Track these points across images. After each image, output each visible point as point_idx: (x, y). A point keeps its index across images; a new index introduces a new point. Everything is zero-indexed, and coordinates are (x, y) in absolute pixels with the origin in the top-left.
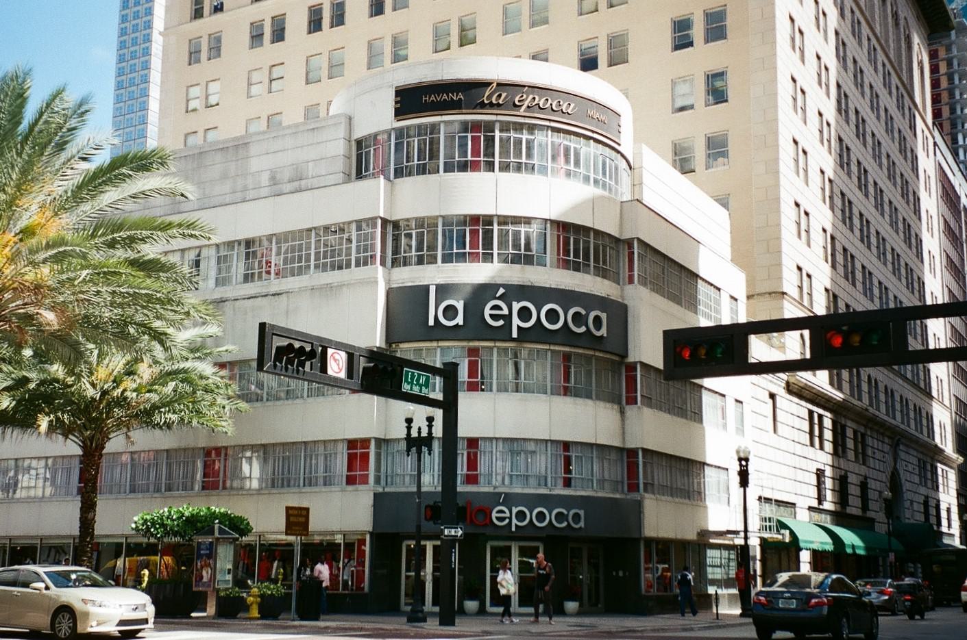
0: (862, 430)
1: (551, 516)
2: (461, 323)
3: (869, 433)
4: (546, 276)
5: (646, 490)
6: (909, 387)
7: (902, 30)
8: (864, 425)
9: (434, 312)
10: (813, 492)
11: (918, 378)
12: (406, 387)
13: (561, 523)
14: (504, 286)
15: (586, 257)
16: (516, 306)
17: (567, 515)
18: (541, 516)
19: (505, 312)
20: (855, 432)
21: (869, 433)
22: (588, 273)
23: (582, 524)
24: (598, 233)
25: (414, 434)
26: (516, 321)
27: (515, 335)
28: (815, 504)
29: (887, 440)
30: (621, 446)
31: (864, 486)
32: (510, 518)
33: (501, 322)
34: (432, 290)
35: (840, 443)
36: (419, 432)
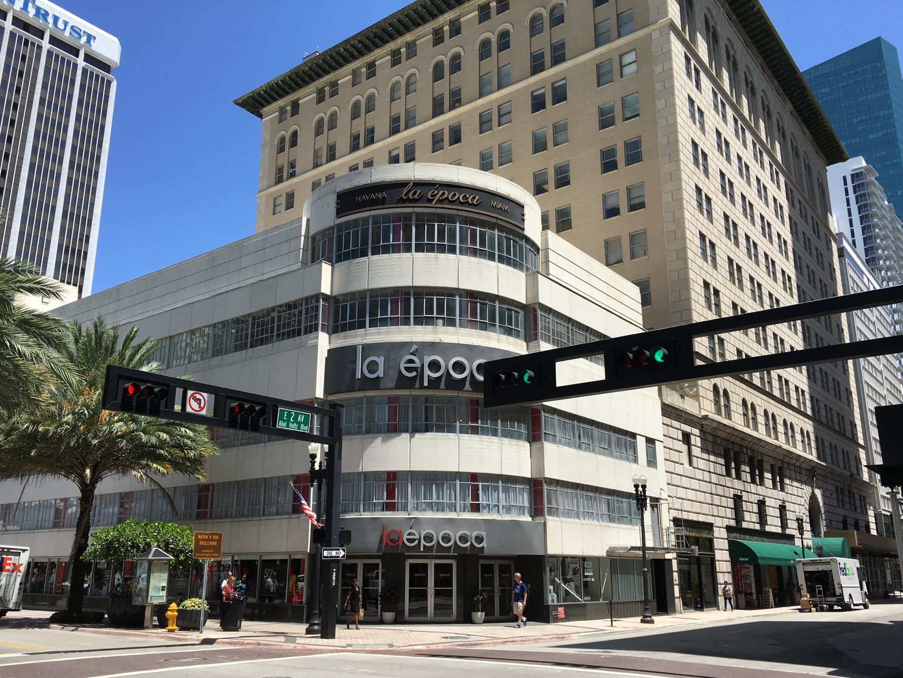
7: (802, 160)
10: (730, 513)
11: (833, 422)
12: (281, 425)
15: (493, 319)
19: (418, 364)
23: (484, 544)
27: (426, 384)
28: (733, 523)
31: (782, 508)
32: (420, 540)
33: (414, 373)
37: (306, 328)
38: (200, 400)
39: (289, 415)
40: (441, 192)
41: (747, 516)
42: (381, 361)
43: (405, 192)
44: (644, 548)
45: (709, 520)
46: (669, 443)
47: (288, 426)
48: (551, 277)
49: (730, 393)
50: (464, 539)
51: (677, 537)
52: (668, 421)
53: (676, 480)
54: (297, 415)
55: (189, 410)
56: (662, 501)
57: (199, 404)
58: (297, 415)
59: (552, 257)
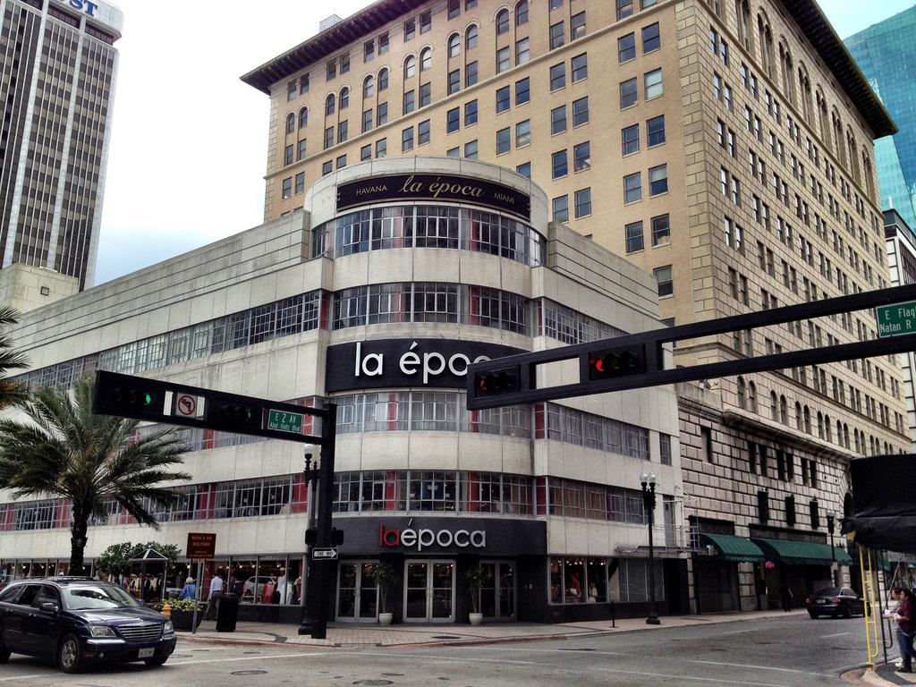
0: (812, 458)
1: (454, 537)
2: (381, 373)
3: (819, 460)
4: (457, 332)
5: (552, 512)
6: (864, 422)
7: (845, 134)
8: (813, 454)
9: (360, 366)
10: (753, 511)
12: (273, 426)
13: (464, 543)
14: (416, 340)
15: (495, 314)
16: (427, 357)
17: (469, 536)
18: (445, 537)
20: (804, 461)
21: (819, 460)
22: (497, 327)
24: (505, 293)
25: (311, 467)
26: (427, 369)
27: (426, 381)
29: (840, 466)
30: (530, 474)
31: (814, 506)
32: (417, 539)
33: (414, 371)
34: (359, 346)
35: (786, 469)
37: (306, 324)
38: (190, 403)
39: (281, 416)
40: (443, 185)
41: (773, 514)
42: (380, 358)
43: (406, 185)
44: (651, 547)
45: (730, 518)
46: (686, 438)
48: (559, 270)
49: (757, 386)
50: (462, 538)
51: (692, 537)
52: (685, 416)
53: (693, 477)
54: (289, 416)
55: (178, 413)
56: (676, 500)
58: (289, 416)
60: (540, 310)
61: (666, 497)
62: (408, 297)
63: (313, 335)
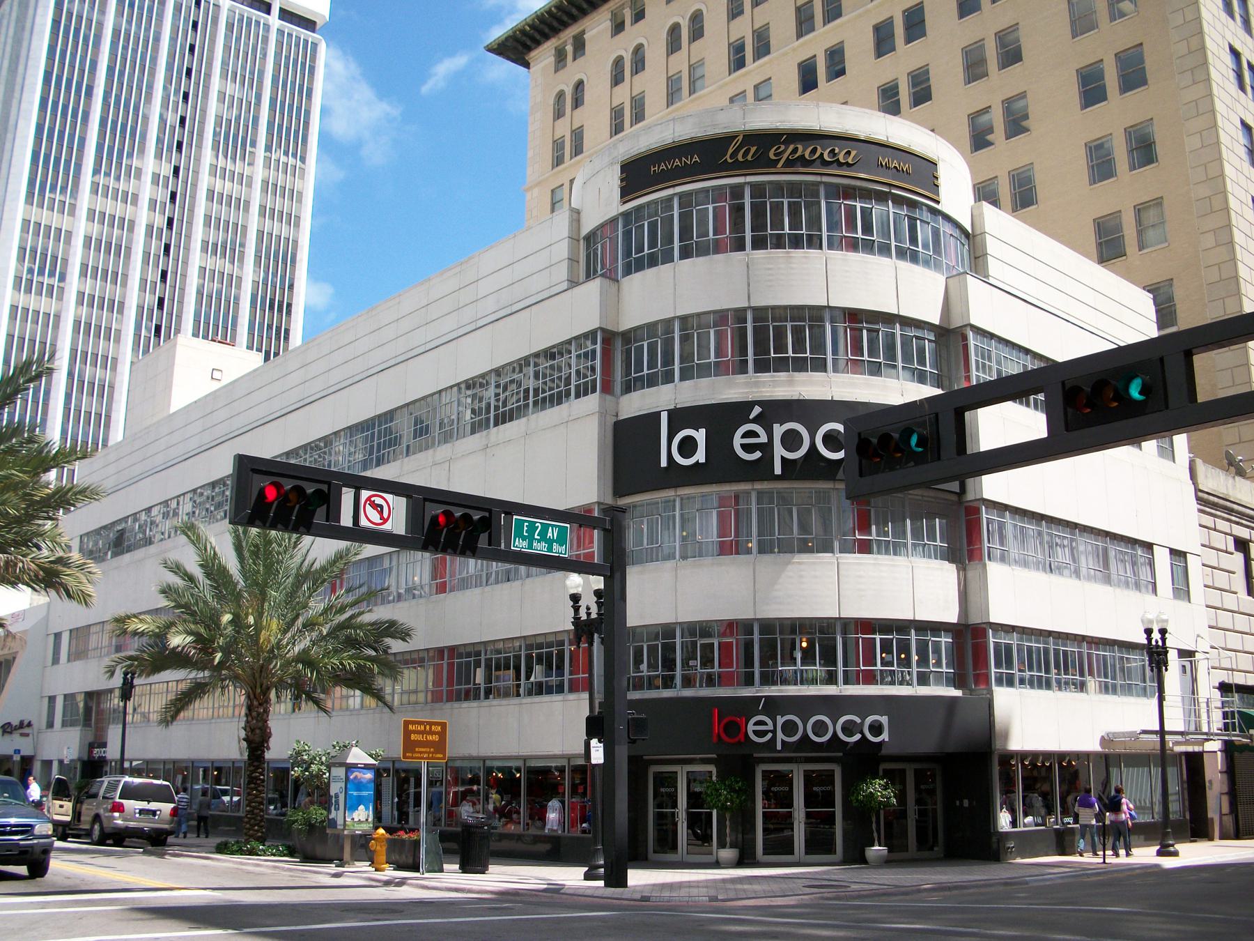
2: (702, 460)
9: (667, 451)
12: (519, 545)
15: (891, 355)
17: (862, 723)
19: (763, 439)
23: (885, 736)
24: (907, 322)
26: (779, 451)
27: (778, 470)
32: (774, 732)
33: (758, 454)
34: (664, 416)
36: (589, 614)
37: (578, 387)
38: (381, 507)
39: (532, 527)
40: (791, 147)
42: (700, 436)
43: (730, 151)
44: (1162, 732)
46: (1211, 557)
47: (530, 546)
48: (991, 281)
50: (849, 729)
51: (1225, 715)
52: (1208, 521)
53: (1225, 619)
54: (545, 528)
57: (381, 513)
58: (545, 528)
59: (992, 246)
60: (966, 347)
61: (1183, 653)
62: (742, 334)
63: (592, 402)
